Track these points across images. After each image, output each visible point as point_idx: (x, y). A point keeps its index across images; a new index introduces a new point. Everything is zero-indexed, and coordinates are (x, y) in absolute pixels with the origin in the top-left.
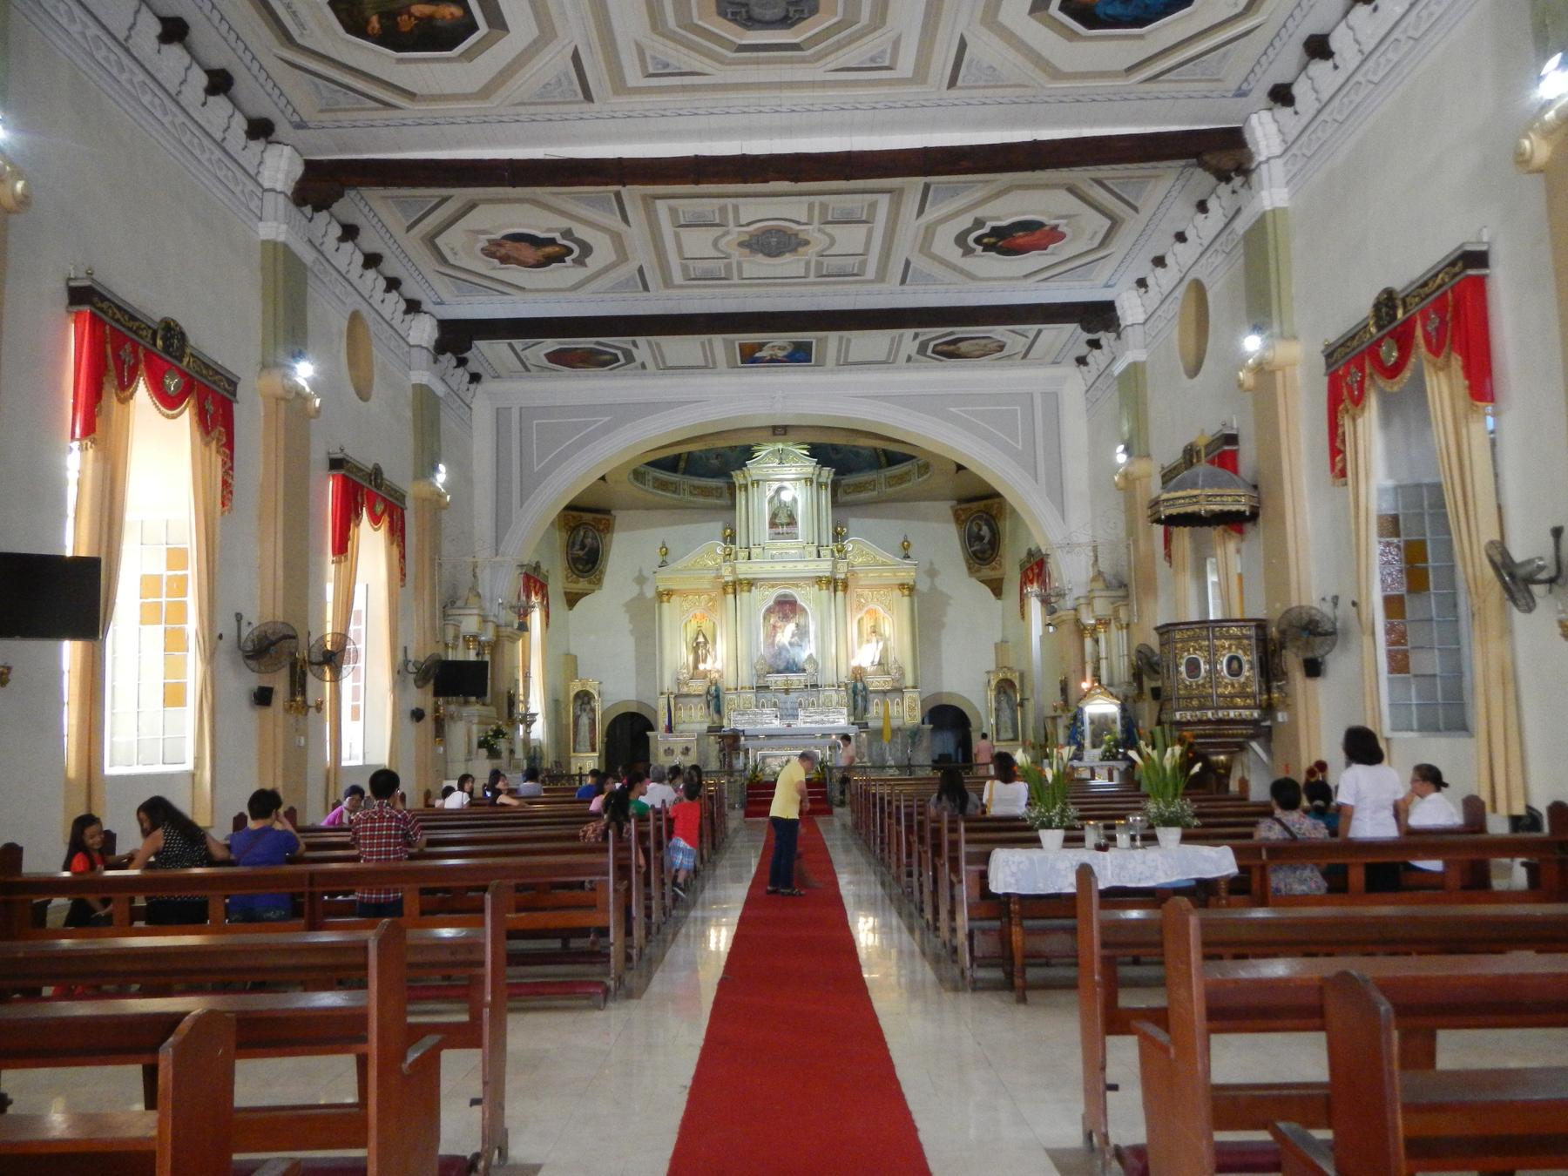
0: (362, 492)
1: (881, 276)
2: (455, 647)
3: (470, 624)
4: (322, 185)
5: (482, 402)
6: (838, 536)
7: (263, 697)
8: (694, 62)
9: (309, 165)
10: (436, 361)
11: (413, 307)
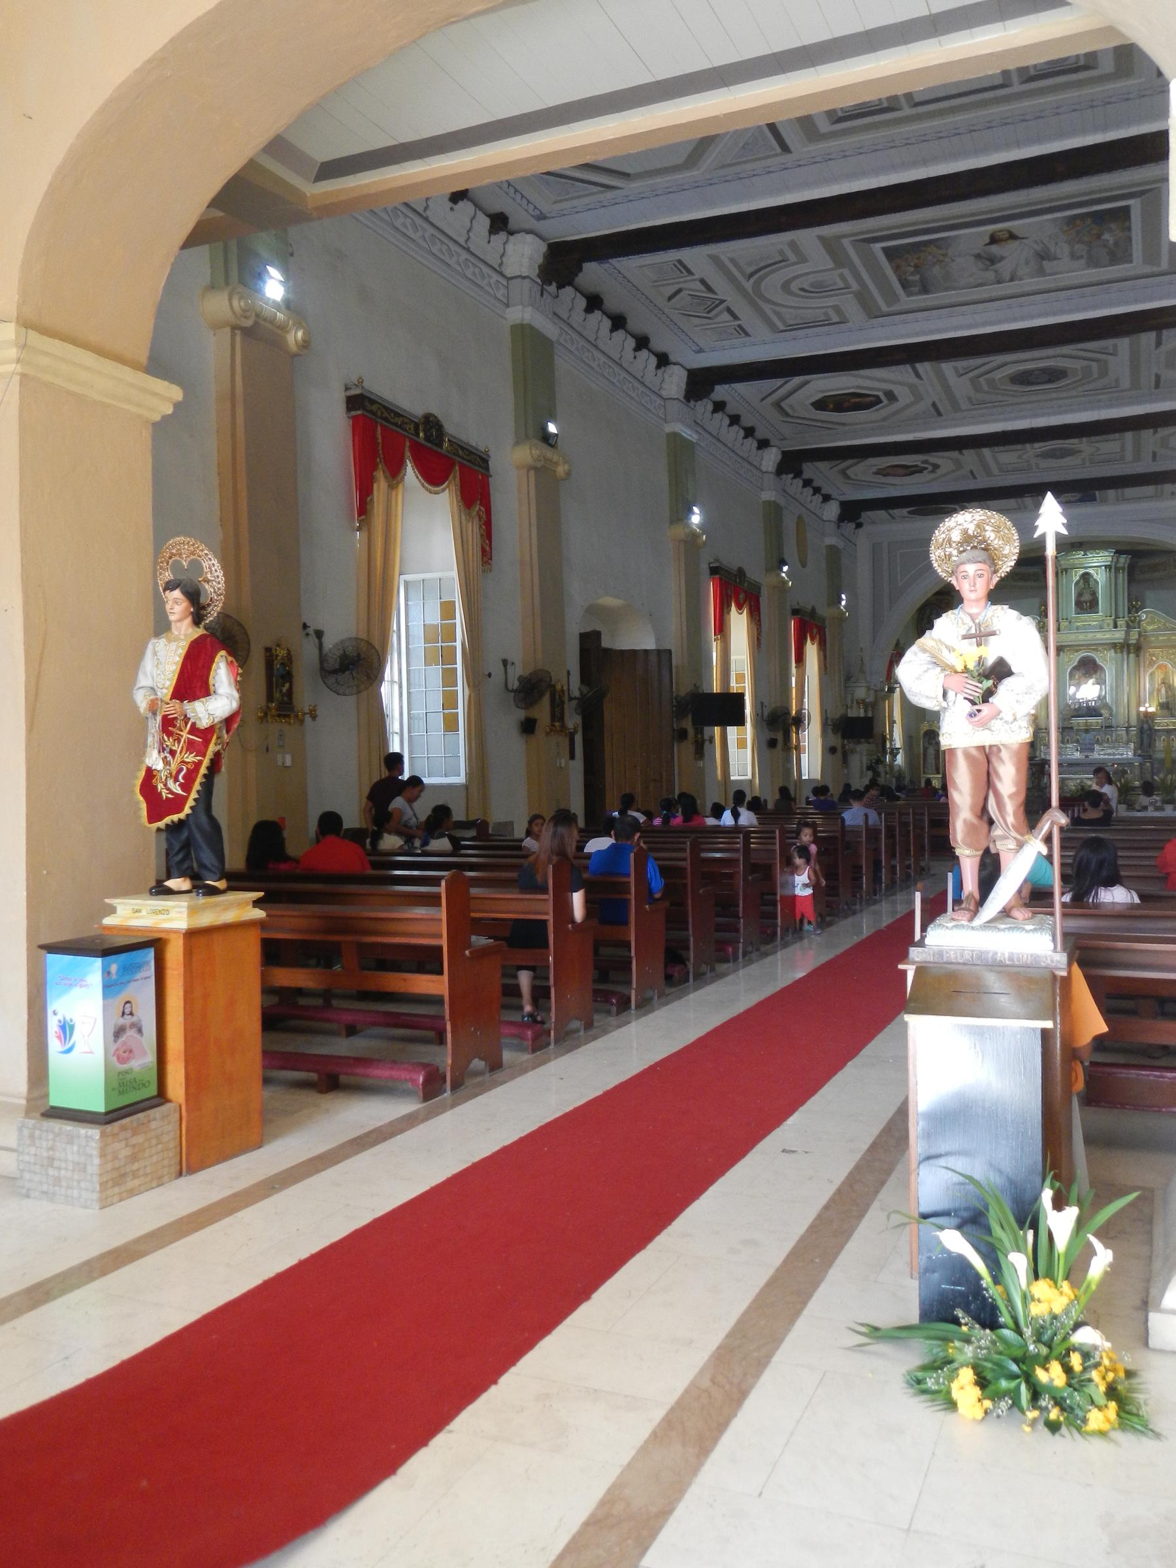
0: (810, 624)
1: (1137, 457)
2: (852, 707)
3: (861, 693)
4: (791, 463)
5: (863, 540)
6: (1133, 609)
7: (772, 743)
8: (1000, 398)
9: (784, 453)
10: (838, 527)
11: (827, 498)
